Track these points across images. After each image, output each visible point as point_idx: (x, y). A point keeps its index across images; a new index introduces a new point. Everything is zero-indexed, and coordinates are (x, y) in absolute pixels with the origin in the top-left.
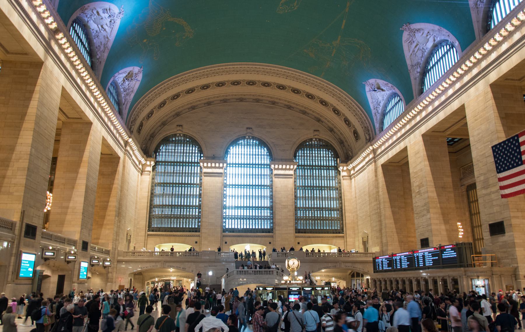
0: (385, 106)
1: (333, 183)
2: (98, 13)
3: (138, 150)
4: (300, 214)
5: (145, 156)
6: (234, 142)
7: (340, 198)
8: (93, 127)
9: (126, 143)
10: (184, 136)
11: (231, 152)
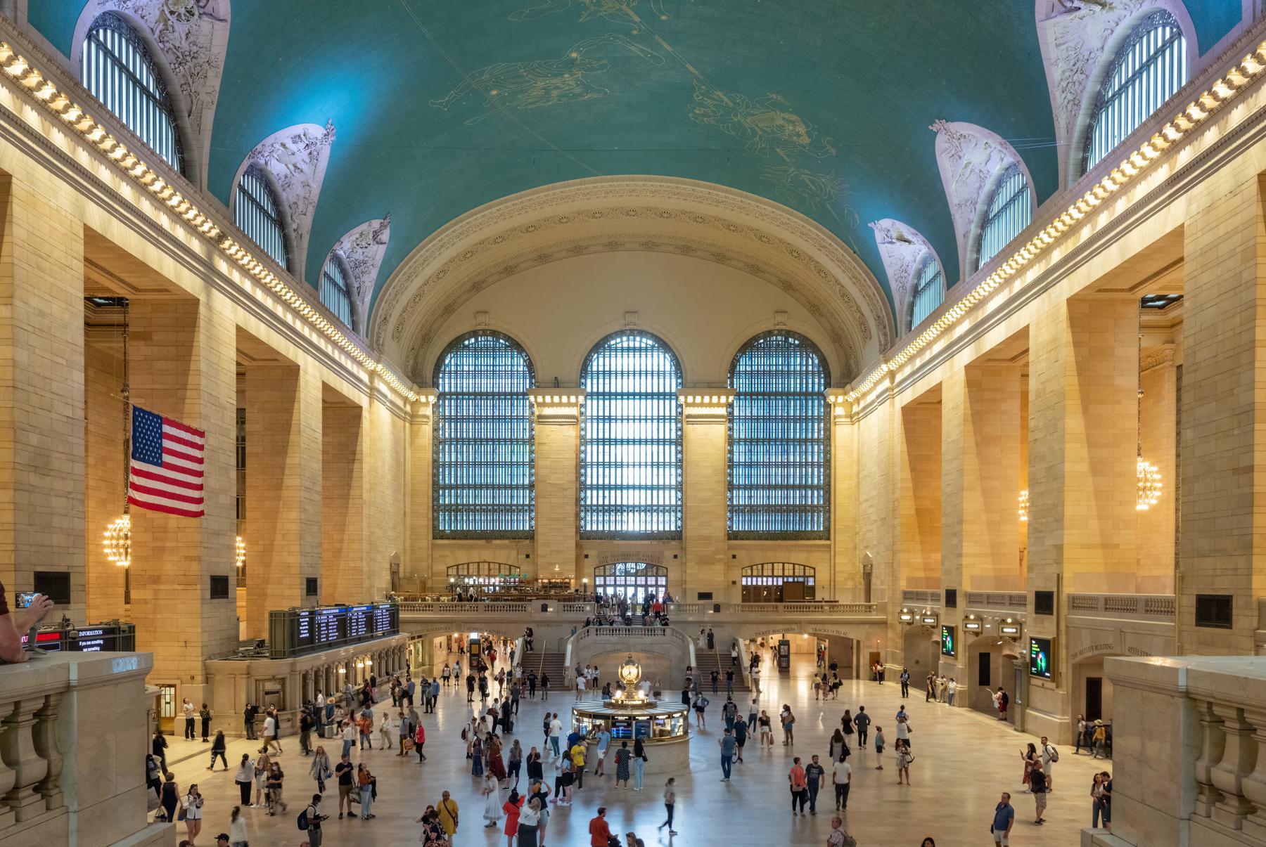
0: (919, 274)
1: (816, 431)
2: (283, 145)
3: (400, 379)
4: (740, 498)
5: (415, 387)
6: (600, 346)
7: (827, 464)
8: (301, 372)
9: (372, 374)
10: (495, 334)
11: (595, 369)
